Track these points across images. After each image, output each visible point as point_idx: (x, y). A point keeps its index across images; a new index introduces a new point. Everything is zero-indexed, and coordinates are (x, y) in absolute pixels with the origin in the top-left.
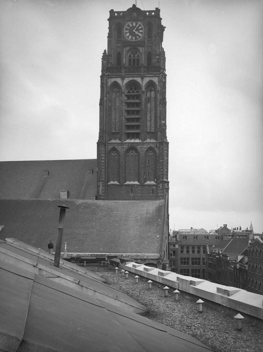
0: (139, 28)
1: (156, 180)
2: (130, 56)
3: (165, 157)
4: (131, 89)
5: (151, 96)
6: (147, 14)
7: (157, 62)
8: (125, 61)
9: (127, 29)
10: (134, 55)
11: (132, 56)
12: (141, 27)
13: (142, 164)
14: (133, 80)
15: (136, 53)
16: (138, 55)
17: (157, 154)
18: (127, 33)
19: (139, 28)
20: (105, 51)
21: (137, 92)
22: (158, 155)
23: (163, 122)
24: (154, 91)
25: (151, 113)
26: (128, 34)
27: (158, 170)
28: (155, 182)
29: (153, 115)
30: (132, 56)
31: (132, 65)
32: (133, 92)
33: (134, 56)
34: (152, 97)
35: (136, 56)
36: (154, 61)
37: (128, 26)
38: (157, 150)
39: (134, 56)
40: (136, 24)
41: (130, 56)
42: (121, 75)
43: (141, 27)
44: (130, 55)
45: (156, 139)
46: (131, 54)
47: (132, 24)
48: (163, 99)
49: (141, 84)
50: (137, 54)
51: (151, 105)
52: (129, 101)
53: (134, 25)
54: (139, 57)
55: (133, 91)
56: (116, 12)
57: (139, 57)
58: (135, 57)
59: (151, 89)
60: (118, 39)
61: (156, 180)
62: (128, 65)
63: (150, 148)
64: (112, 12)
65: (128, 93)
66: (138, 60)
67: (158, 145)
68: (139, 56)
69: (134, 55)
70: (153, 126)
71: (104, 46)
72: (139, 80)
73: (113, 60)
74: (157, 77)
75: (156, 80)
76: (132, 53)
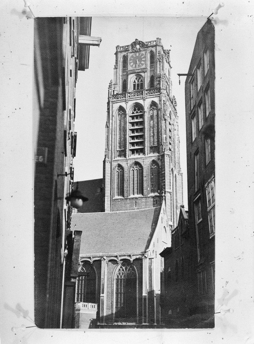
0: (142, 57)
1: (159, 191)
2: (135, 82)
3: (167, 168)
4: (135, 110)
5: (153, 114)
6: (149, 43)
7: (158, 84)
8: (130, 88)
9: (130, 60)
10: (138, 80)
11: (136, 81)
12: (143, 56)
13: (145, 177)
14: (136, 103)
16: (142, 80)
17: (160, 166)
18: (130, 63)
19: (142, 57)
21: (141, 112)
22: (160, 167)
24: (156, 109)
25: (153, 129)
26: (132, 64)
27: (161, 182)
28: (158, 193)
29: (156, 131)
30: (136, 81)
31: (136, 89)
32: (137, 112)
34: (154, 115)
35: (140, 81)
36: (156, 83)
38: (160, 163)
40: (139, 54)
42: (126, 99)
43: (143, 56)
45: (159, 153)
46: (136, 80)
47: (136, 55)
48: (164, 115)
49: (143, 105)
50: (141, 79)
51: (153, 122)
54: (143, 82)
55: (137, 112)
56: (123, 47)
57: (143, 82)
59: (153, 108)
60: (124, 68)
61: (159, 191)
62: (133, 90)
63: (154, 162)
65: (132, 114)
67: (160, 157)
68: (143, 80)
70: (156, 140)
72: (141, 102)
73: (119, 89)
74: (158, 97)
75: (156, 100)
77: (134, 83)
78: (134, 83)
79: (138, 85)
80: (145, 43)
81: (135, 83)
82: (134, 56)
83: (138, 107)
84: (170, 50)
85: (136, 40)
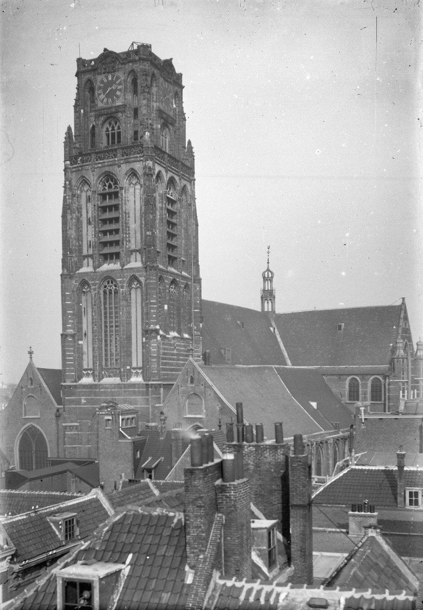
2: (108, 130)
9: (100, 88)
10: (113, 128)
12: (119, 81)
15: (116, 123)
18: (100, 94)
20: (69, 128)
23: (148, 233)
33: (113, 129)
35: (116, 128)
37: (102, 82)
39: (113, 129)
40: (112, 78)
41: (108, 130)
44: (107, 129)
47: (107, 78)
50: (117, 125)
52: (104, 204)
53: (110, 78)
58: (114, 130)
64: (80, 62)
66: (119, 134)
69: (113, 128)
71: (69, 119)
76: (110, 124)
77: (106, 132)
78: (106, 132)
79: (113, 135)
80: (121, 55)
81: (108, 132)
82: (105, 81)
83: (109, 177)
84: (171, 59)
85: (105, 50)
